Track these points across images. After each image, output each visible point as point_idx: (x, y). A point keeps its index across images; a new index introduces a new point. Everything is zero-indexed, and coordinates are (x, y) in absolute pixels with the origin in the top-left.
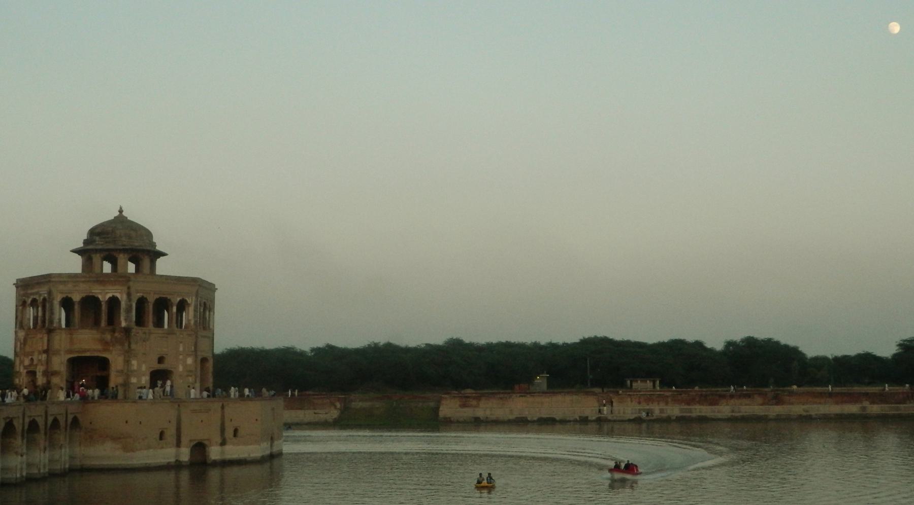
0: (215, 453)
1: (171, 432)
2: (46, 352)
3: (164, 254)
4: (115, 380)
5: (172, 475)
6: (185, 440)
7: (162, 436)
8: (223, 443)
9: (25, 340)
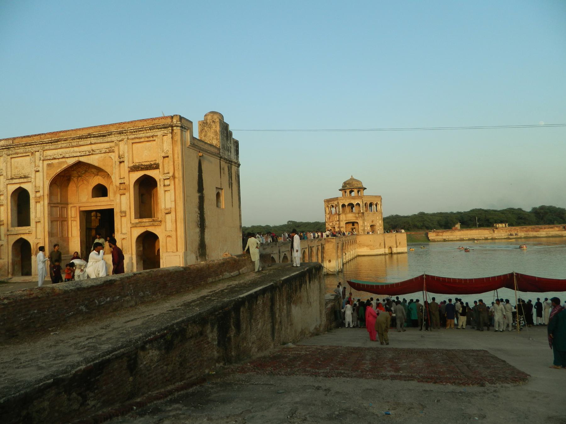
1: (383, 244)
2: (339, 221)
5: (384, 257)
8: (397, 247)
9: (329, 218)
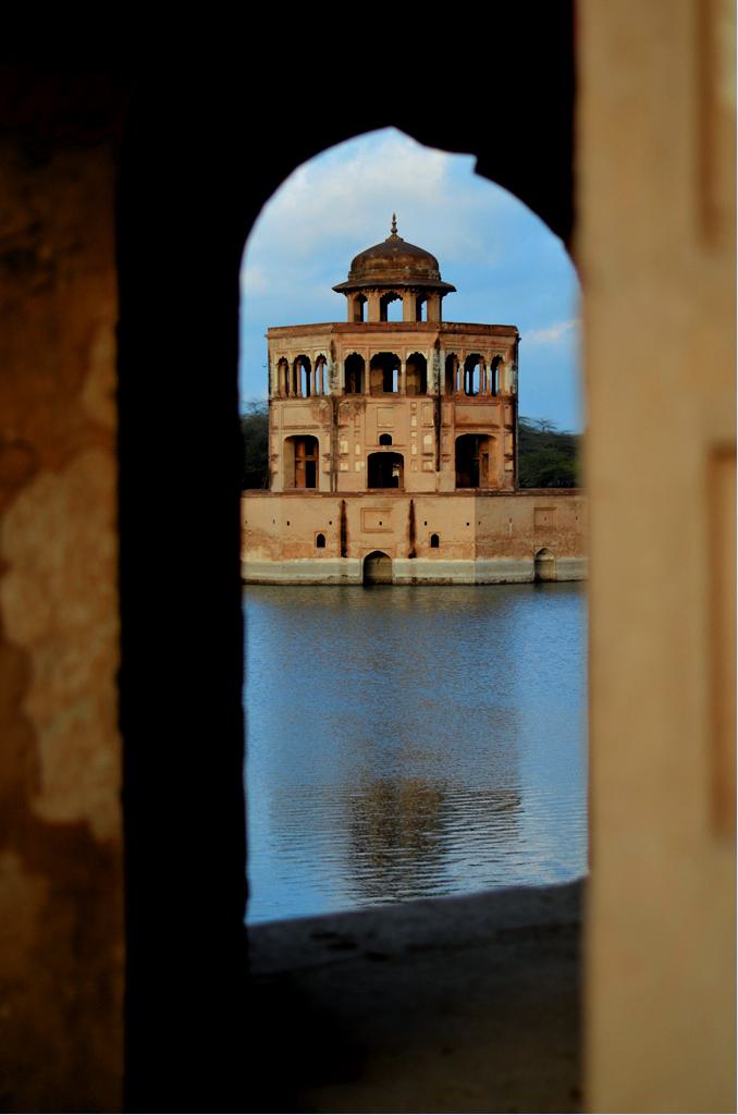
0: (401, 567)
3: (452, 289)
4: (324, 466)
6: (351, 545)
7: (321, 541)
8: (413, 555)
